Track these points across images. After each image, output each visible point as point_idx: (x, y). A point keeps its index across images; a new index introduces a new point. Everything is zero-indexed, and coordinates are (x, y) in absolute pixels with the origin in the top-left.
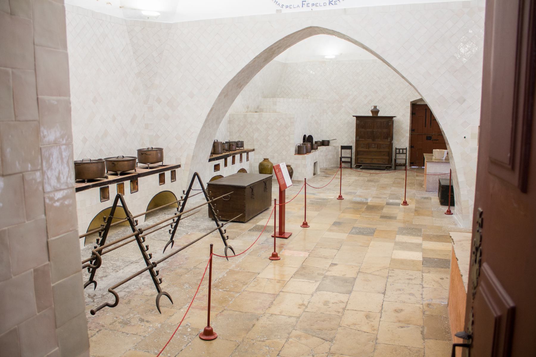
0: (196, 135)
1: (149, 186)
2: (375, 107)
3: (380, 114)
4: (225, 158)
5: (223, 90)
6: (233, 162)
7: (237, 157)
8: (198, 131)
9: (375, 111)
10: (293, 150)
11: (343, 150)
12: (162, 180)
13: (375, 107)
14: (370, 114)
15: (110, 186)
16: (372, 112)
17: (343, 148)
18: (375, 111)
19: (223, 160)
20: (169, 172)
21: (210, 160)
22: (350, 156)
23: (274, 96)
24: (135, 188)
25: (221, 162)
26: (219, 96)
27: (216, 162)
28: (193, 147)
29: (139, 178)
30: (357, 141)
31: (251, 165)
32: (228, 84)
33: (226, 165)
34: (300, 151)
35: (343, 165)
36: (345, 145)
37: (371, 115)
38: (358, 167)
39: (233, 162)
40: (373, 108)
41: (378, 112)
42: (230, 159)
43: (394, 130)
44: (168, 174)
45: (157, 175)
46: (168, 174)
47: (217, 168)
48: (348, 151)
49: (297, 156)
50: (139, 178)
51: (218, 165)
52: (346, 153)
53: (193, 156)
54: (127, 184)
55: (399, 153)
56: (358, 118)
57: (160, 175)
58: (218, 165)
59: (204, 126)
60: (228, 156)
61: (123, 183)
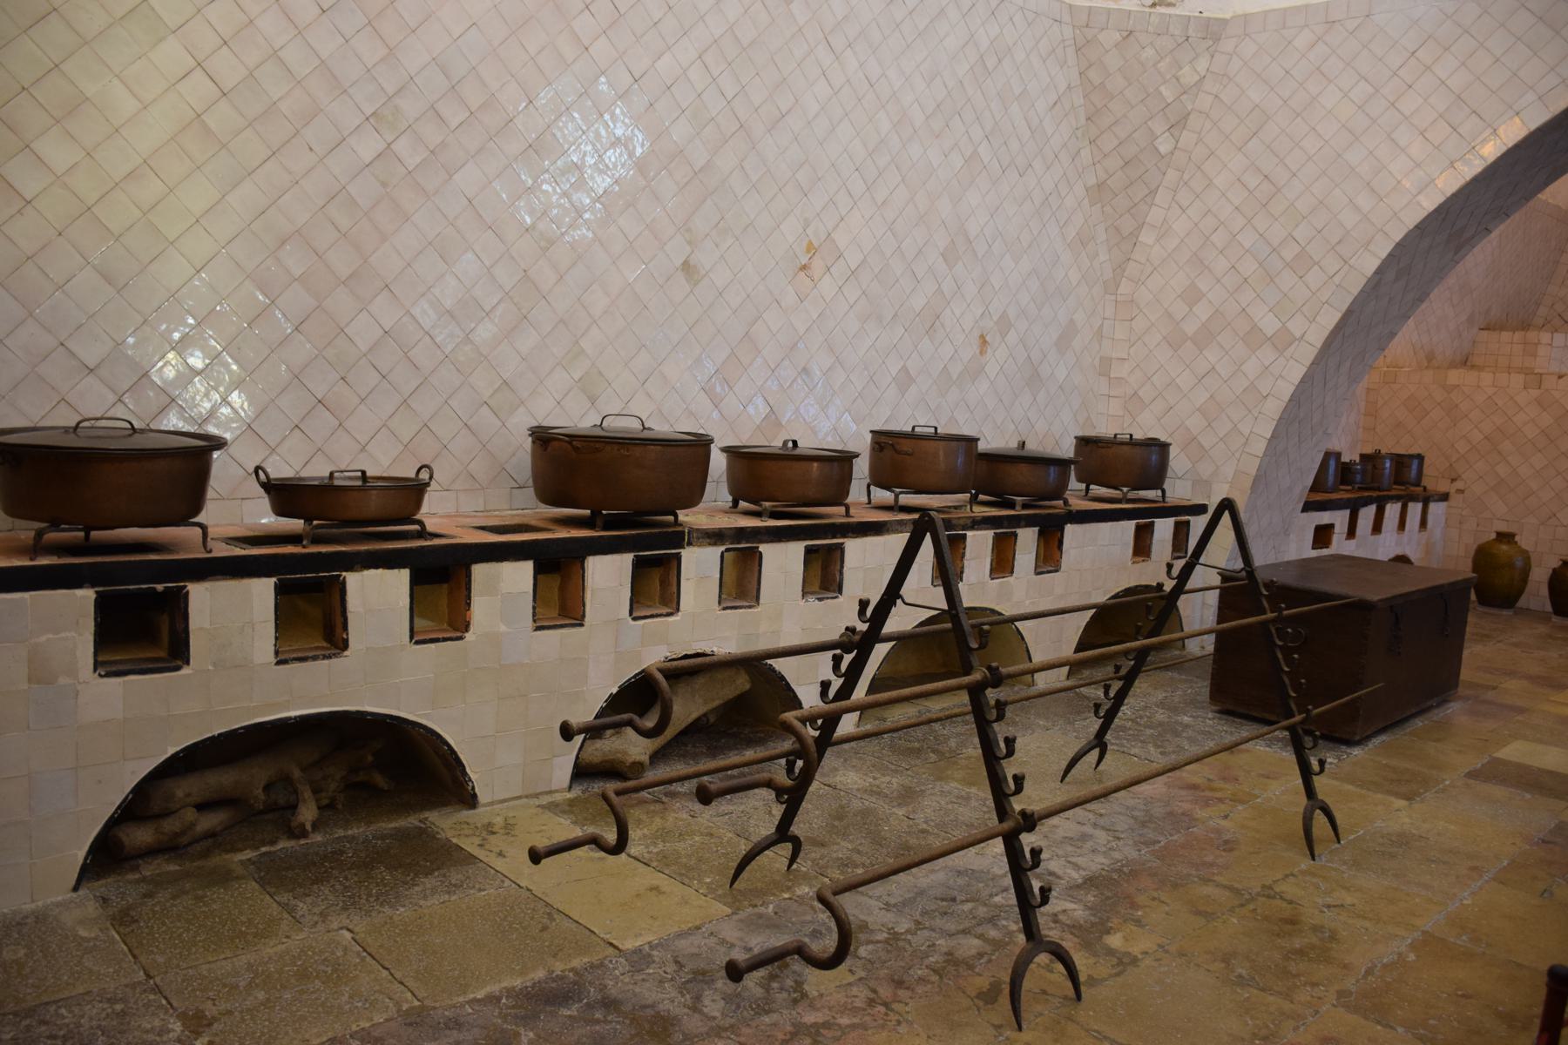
0: (1274, 408)
1: (1100, 560)
4: (1354, 508)
5: (1399, 245)
6: (1377, 528)
7: (1392, 510)
8: (1286, 390)
12: (1142, 547)
15: (969, 534)
19: (1347, 512)
20: (1170, 521)
21: (1308, 507)
23: (1525, 326)
24: (1049, 558)
25: (1339, 519)
26: (1380, 271)
27: (1325, 517)
28: (1259, 447)
29: (1069, 528)
32: (1421, 229)
33: (1351, 533)
39: (1377, 528)
42: (1367, 514)
44: (1164, 528)
45: (1130, 525)
46: (1164, 528)
47: (1322, 535)
50: (1069, 528)
51: (1332, 526)
53: (1256, 480)
54: (1027, 538)
57: (1138, 528)
58: (1332, 526)
59: (1306, 380)
60: (1366, 502)
61: (1015, 535)
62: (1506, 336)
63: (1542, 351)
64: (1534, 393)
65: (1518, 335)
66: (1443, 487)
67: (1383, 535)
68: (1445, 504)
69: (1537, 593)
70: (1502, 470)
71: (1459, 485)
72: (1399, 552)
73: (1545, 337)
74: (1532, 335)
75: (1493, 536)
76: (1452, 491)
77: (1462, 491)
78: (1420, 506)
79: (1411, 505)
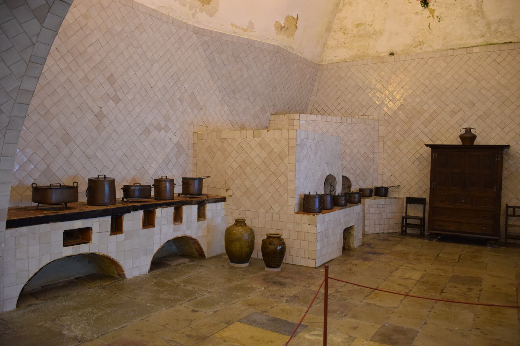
2: (468, 130)
3: (479, 141)
9: (468, 137)
10: (293, 203)
11: (408, 205)
13: (468, 130)
14: (458, 142)
16: (462, 137)
17: (410, 200)
18: (468, 137)
22: (421, 215)
27: (78, 224)
30: (432, 190)
31: (210, 229)
34: (308, 205)
35: (409, 231)
36: (416, 196)
37: (461, 144)
38: (432, 237)
40: (463, 131)
41: (474, 137)
43: (505, 173)
48: (420, 207)
49: (299, 216)
52: (416, 211)
55: (514, 215)
56: (434, 148)
62: (281, 116)
63: (296, 123)
64: (258, 140)
65: (286, 116)
66: (223, 195)
67: (156, 229)
68: (223, 203)
69: (257, 254)
70: (247, 184)
71: (230, 193)
72: (179, 234)
73: (297, 116)
74: (292, 116)
75: (234, 222)
76: (227, 196)
77: (230, 196)
78: (195, 207)
79: (185, 208)
